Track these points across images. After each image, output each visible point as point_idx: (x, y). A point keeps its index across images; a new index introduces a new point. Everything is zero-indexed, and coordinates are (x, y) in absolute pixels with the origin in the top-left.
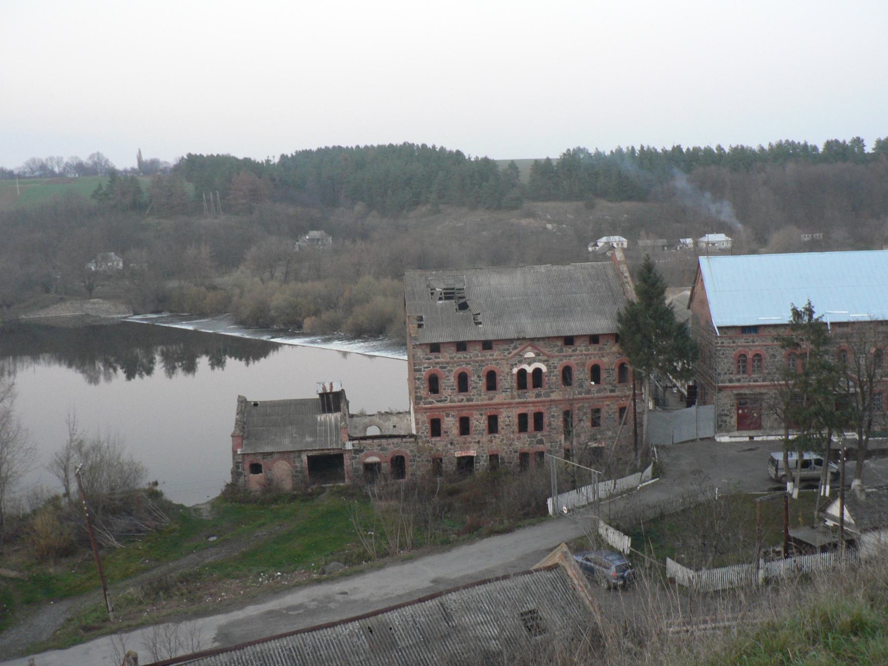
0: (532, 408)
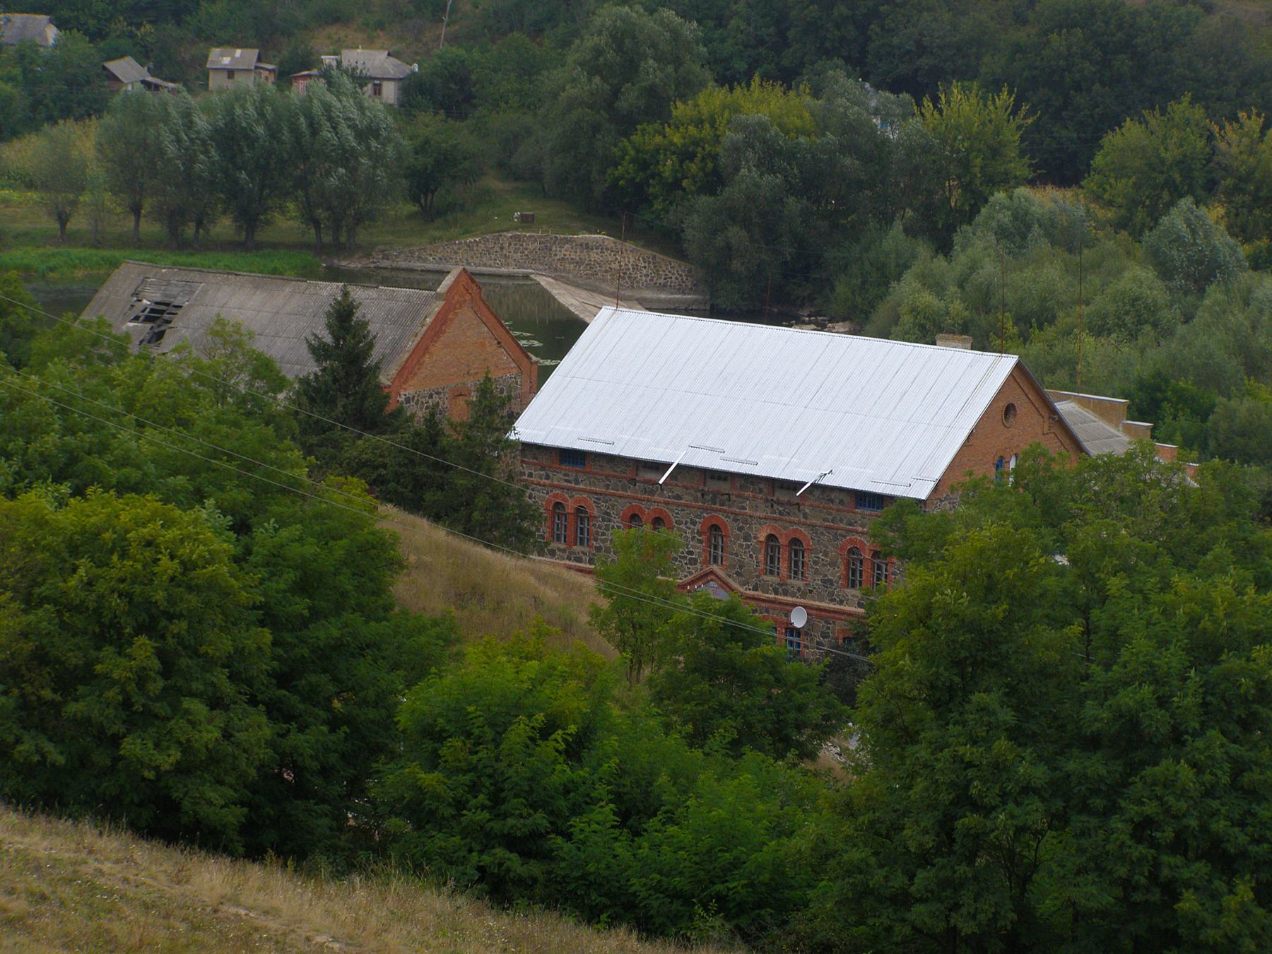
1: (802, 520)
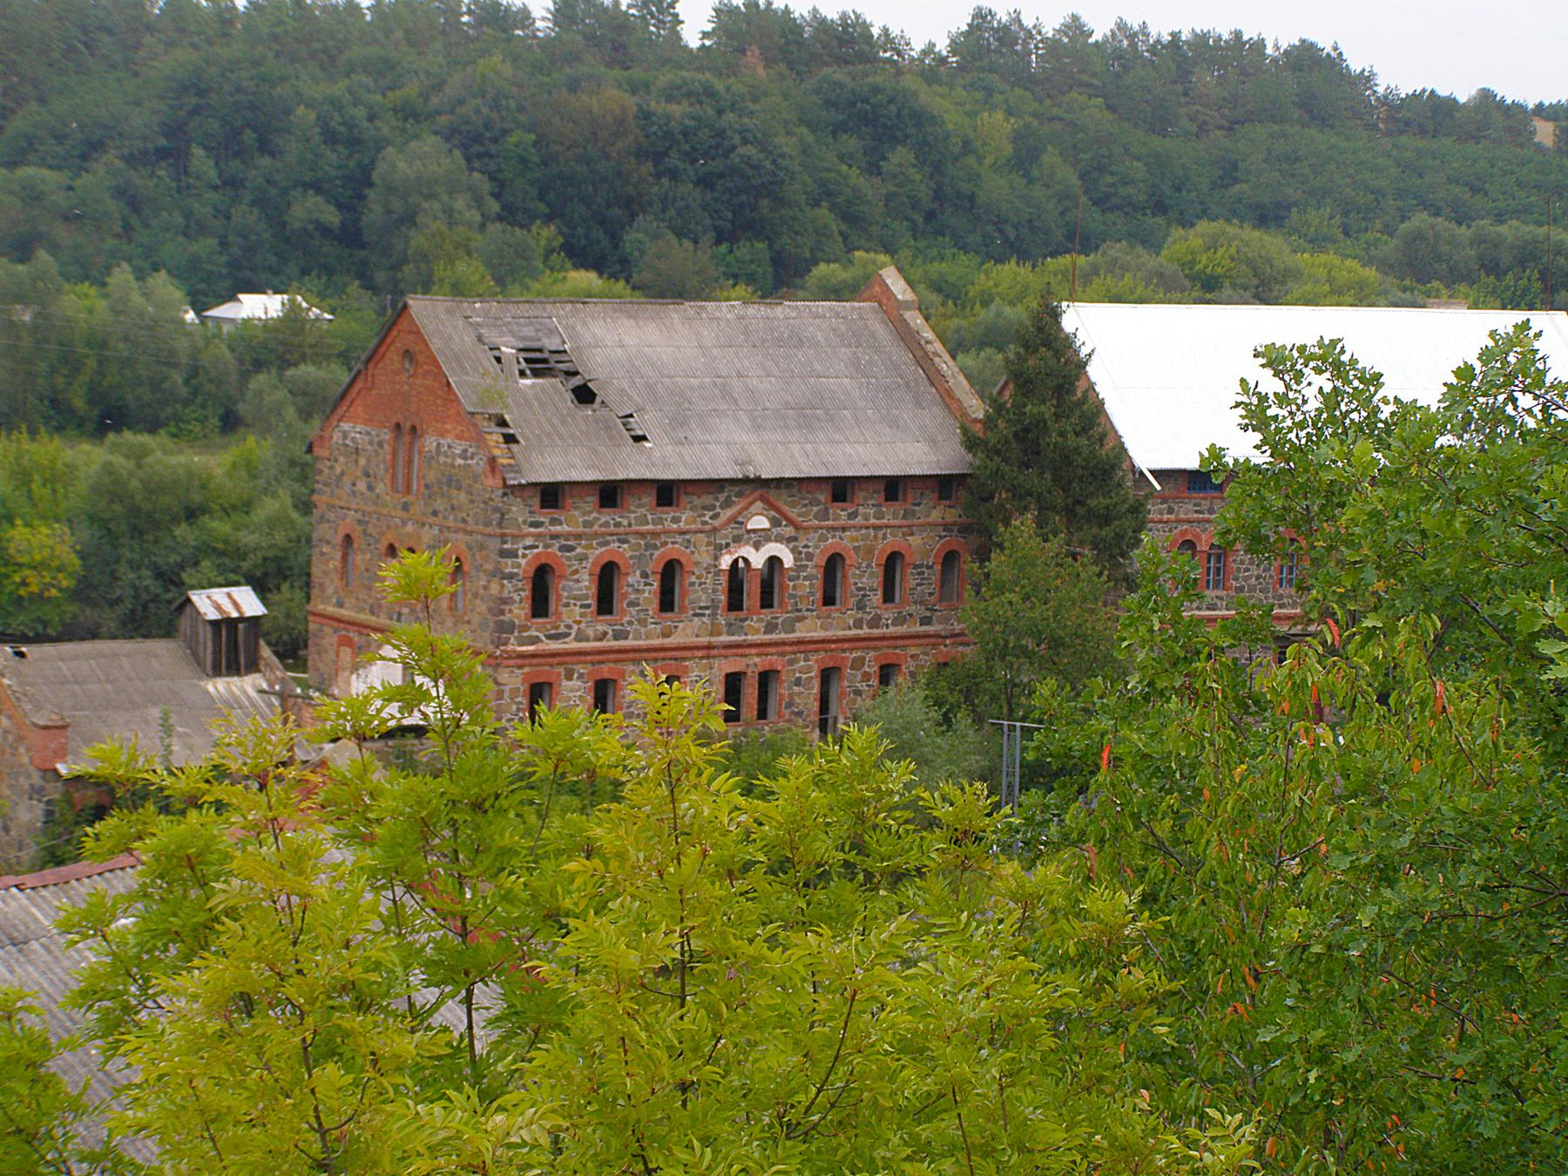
0: (757, 660)
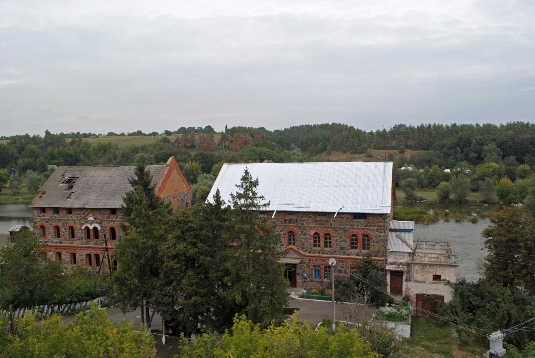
0: (93, 251)
1: (330, 226)
